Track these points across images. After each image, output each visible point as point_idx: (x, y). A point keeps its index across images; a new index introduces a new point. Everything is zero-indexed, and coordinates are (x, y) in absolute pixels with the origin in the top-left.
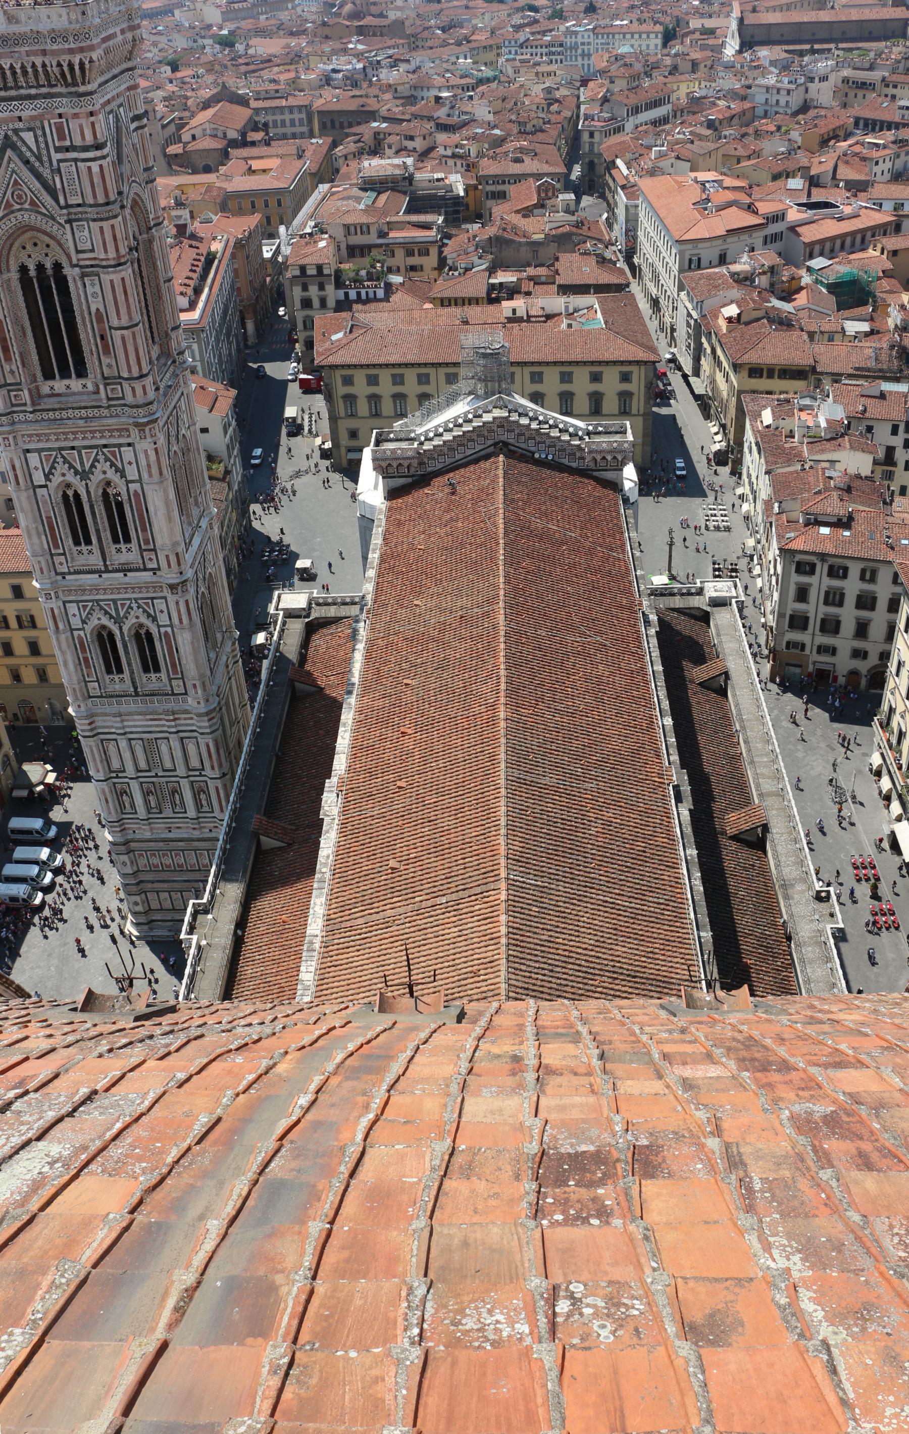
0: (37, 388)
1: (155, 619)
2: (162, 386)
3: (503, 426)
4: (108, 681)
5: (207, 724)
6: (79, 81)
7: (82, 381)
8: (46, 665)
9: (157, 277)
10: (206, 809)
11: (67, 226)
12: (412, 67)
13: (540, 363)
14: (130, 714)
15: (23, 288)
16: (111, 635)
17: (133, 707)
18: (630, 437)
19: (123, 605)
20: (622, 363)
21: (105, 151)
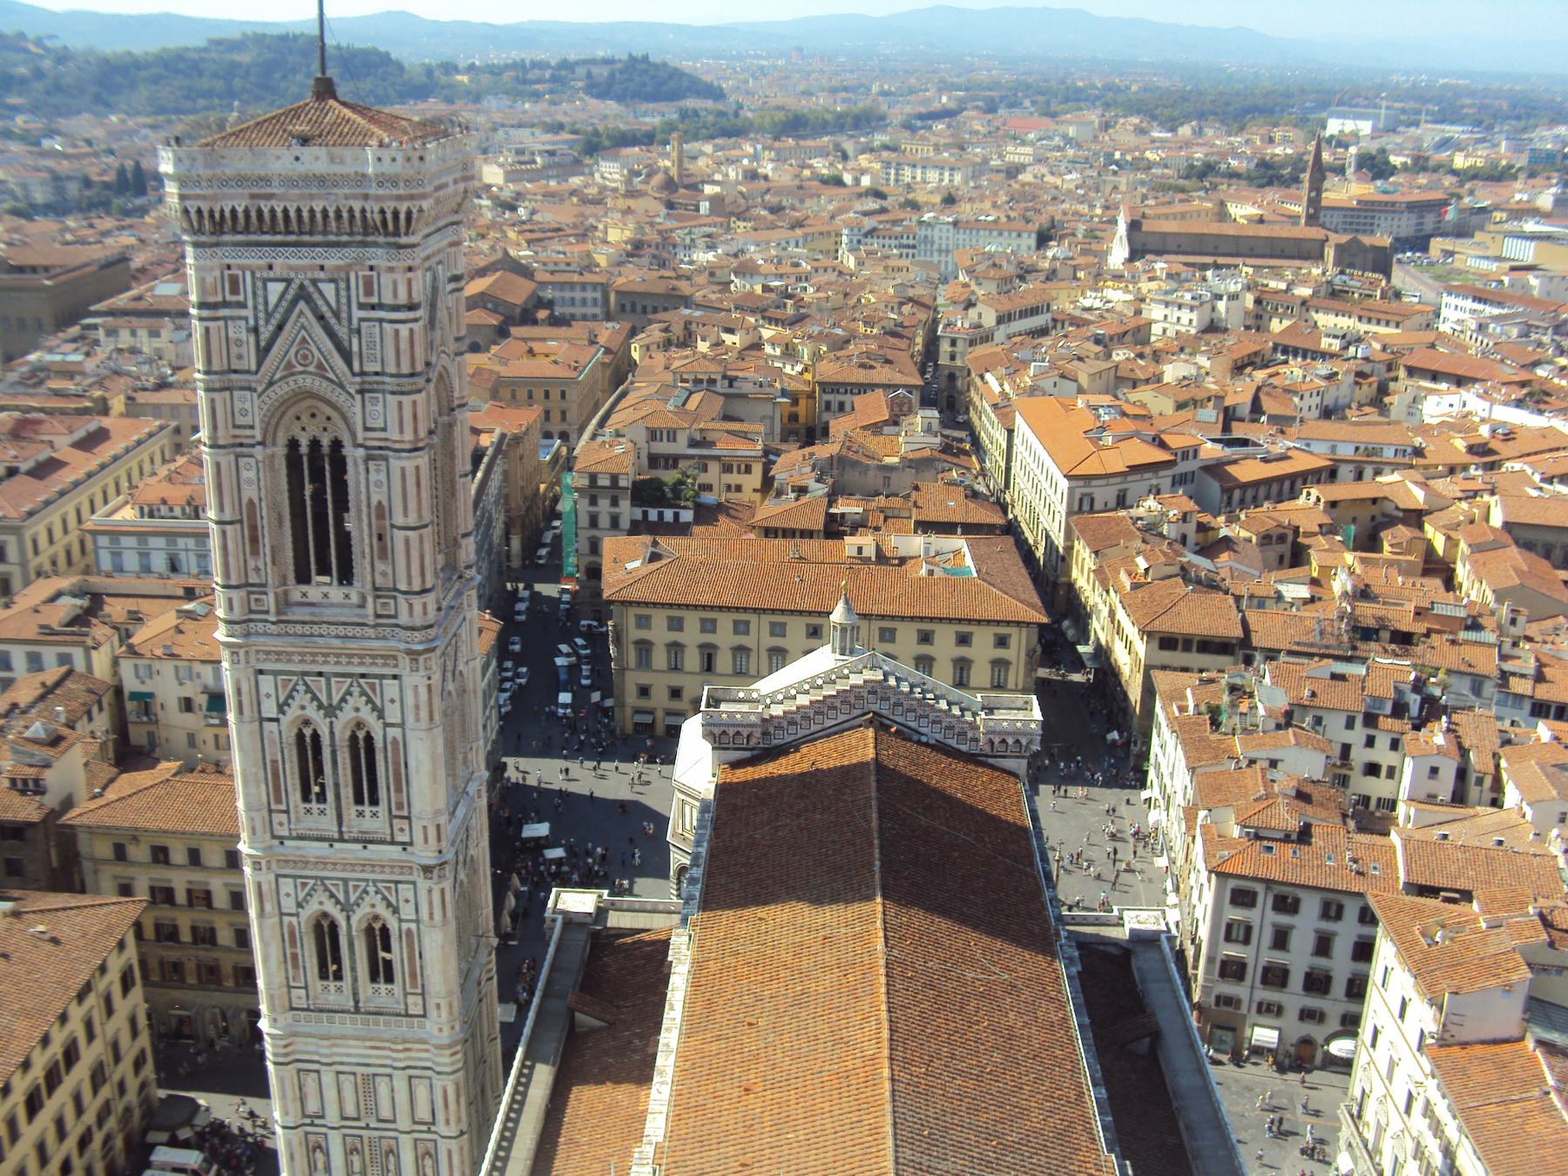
0: (286, 593)
1: (396, 911)
2: (444, 604)
3: (875, 693)
4: (319, 988)
6: (403, 230)
7: (346, 590)
11: (358, 397)
14: (344, 1037)
16: (333, 927)
18: (1037, 714)
20: (998, 623)
21: (419, 313)
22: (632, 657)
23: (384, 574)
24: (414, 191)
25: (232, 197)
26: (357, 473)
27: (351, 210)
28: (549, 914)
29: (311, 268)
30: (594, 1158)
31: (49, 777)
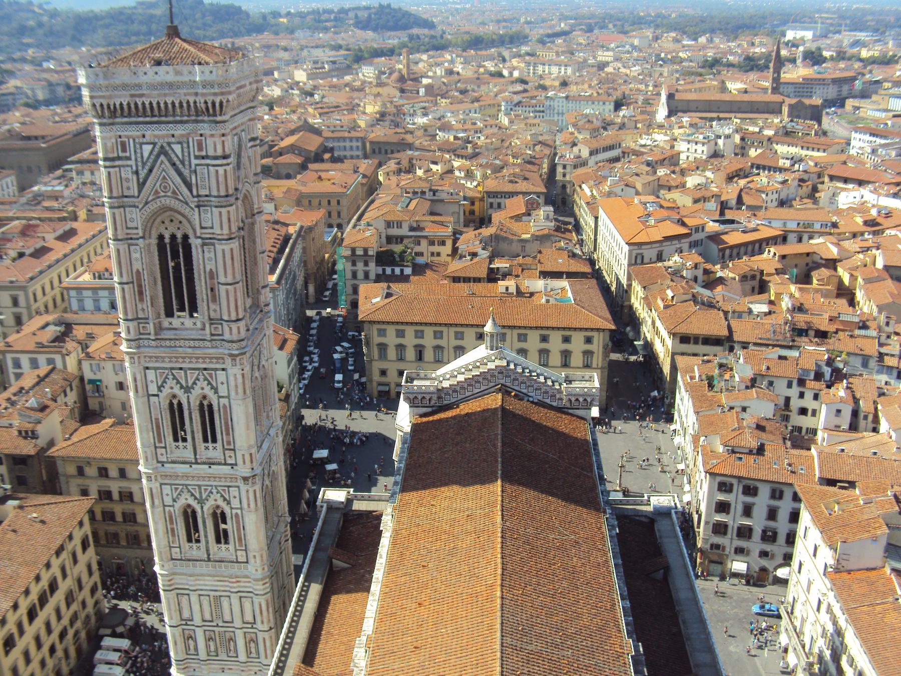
0: (160, 323)
1: (229, 503)
2: (251, 328)
3: (502, 373)
4: (187, 548)
5: (262, 587)
6: (218, 112)
9: (255, 249)
10: (254, 655)
11: (196, 210)
13: (525, 328)
15: (159, 251)
16: (194, 512)
18: (597, 384)
20: (586, 329)
21: (229, 161)
22: (376, 353)
23: (215, 311)
24: (224, 90)
25: (120, 97)
26: (198, 253)
27: (188, 102)
28: (318, 503)
29: (167, 136)
30: (341, 643)
31: (40, 429)
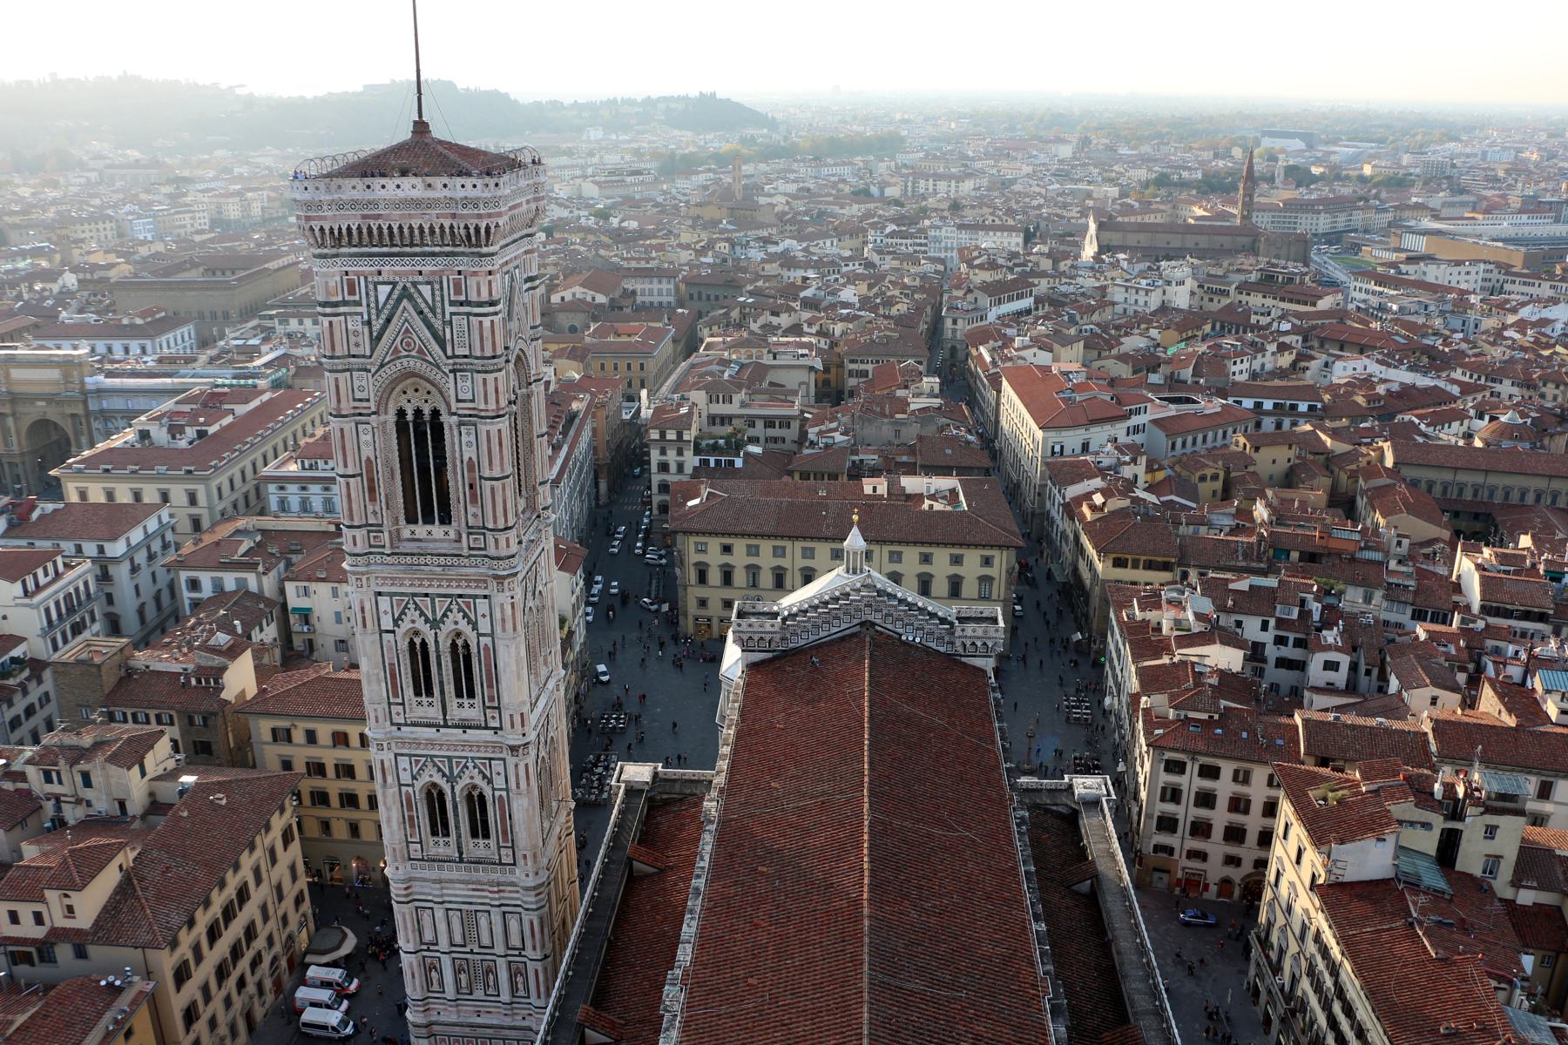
0: (398, 531)
1: (490, 782)
2: (525, 539)
3: (871, 606)
4: (431, 843)
5: (533, 899)
7: (446, 528)
8: (358, 821)
10: (521, 993)
11: (451, 375)
12: (779, 249)
14: (451, 881)
16: (441, 794)
17: (455, 875)
19: (458, 763)
21: (498, 308)
26: (452, 435)
27: (442, 226)
29: (412, 273)
